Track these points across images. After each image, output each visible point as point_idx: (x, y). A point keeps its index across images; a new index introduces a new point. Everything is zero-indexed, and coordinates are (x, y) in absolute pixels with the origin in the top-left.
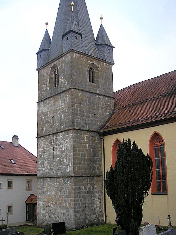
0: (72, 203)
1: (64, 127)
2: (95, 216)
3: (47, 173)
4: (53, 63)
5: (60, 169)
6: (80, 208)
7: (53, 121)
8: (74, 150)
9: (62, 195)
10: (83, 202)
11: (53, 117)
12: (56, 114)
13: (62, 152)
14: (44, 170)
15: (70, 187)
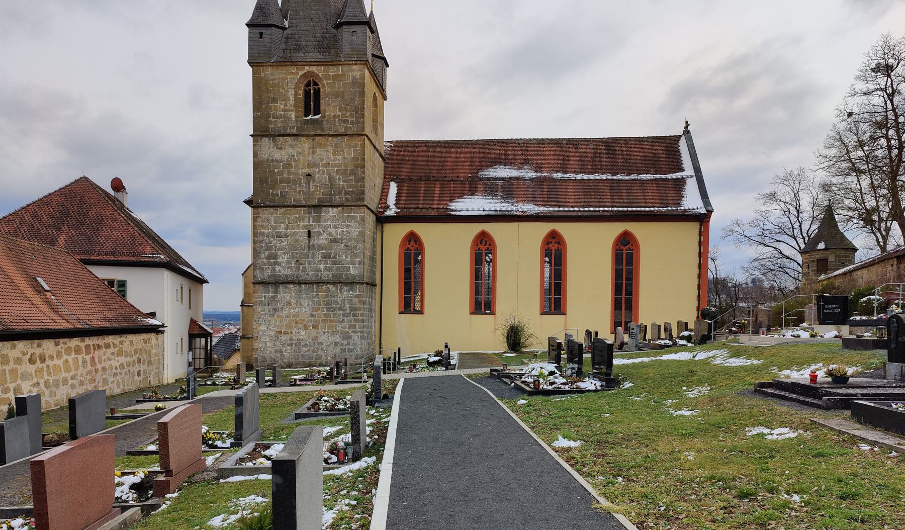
3: (286, 276)
4: (307, 68)
5: (326, 269)
11: (309, 175)
13: (335, 241)
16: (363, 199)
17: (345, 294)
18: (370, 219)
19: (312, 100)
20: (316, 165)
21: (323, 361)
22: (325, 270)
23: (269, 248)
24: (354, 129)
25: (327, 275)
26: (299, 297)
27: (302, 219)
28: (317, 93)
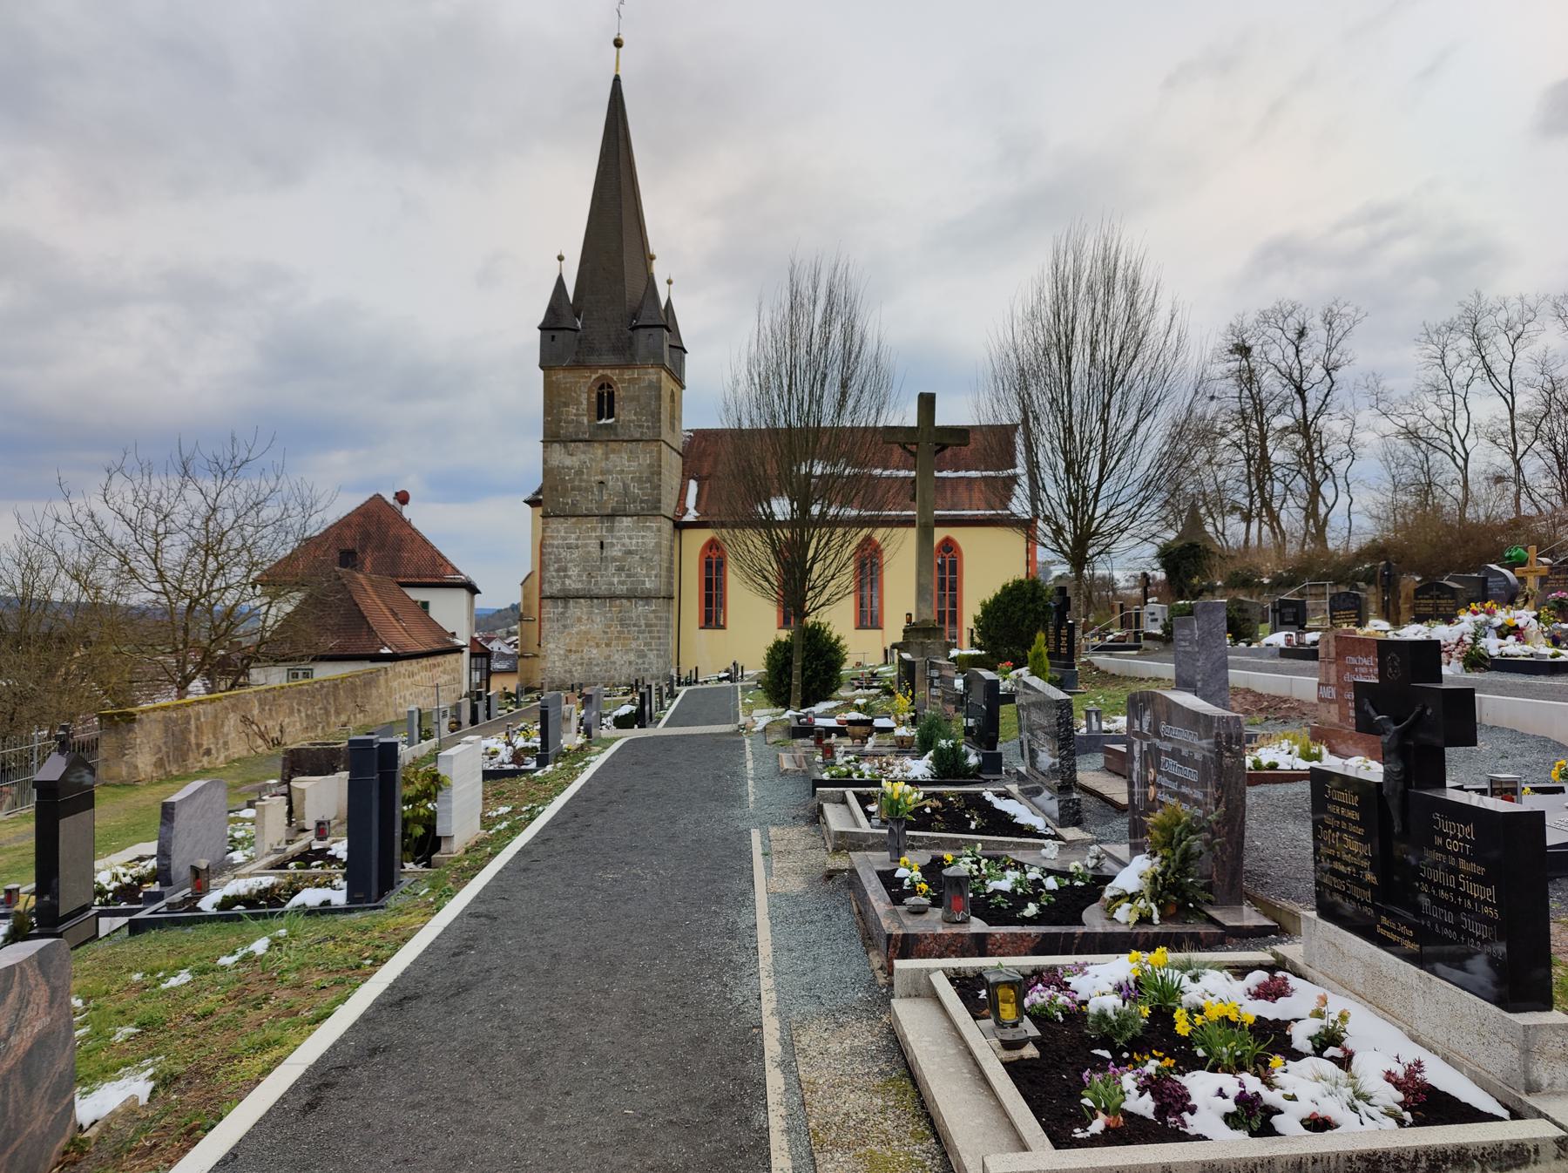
5: (620, 582)
13: (630, 552)
16: (659, 508)
17: (641, 608)
18: (667, 526)
19: (605, 403)
20: (609, 472)
21: (616, 681)
22: (618, 583)
23: (558, 560)
24: (649, 434)
25: (621, 589)
27: (594, 529)
28: (611, 395)
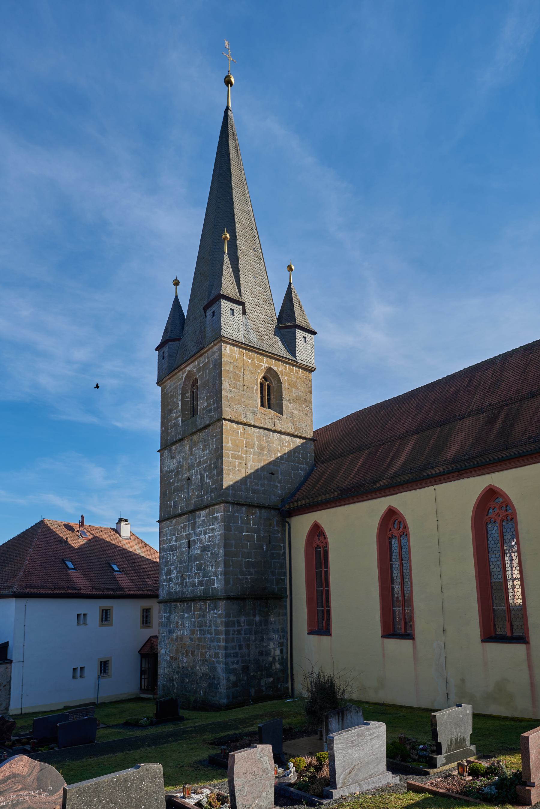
0: (222, 652)
1: (207, 498)
2: (271, 679)
3: (176, 592)
4: (187, 368)
5: (200, 583)
6: (237, 663)
7: (188, 489)
8: (225, 546)
9: (203, 636)
10: (245, 650)
11: (189, 479)
12: (194, 472)
13: (204, 549)
14: (171, 586)
15: (219, 621)
26: (183, 618)
